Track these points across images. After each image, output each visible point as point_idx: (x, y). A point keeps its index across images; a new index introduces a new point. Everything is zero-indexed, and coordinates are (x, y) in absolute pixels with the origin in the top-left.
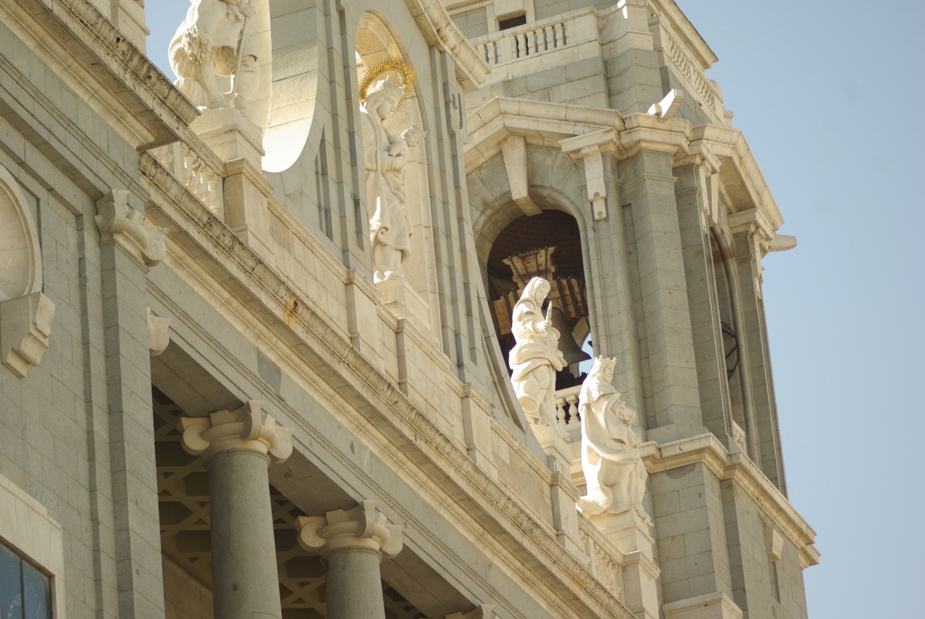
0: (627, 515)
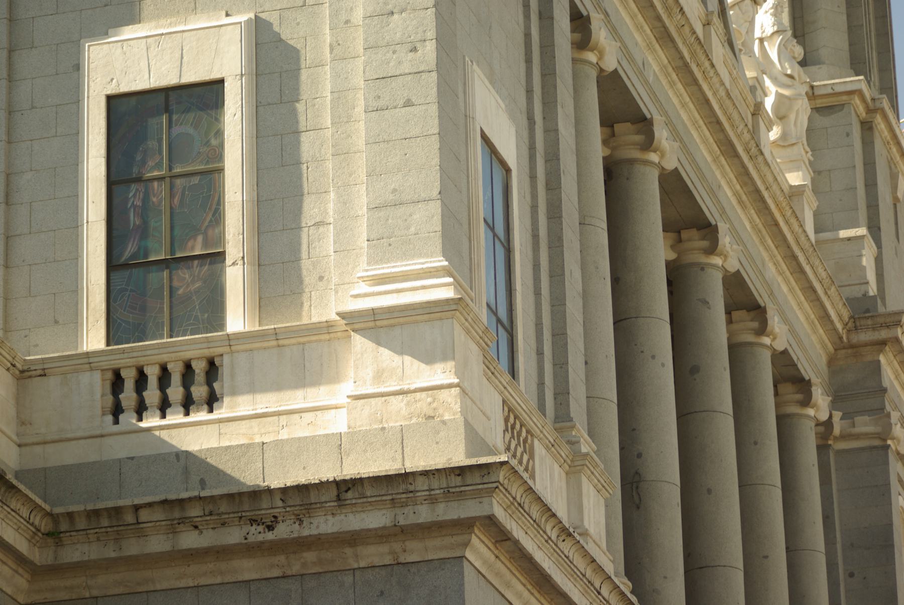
0: (795, 147)
